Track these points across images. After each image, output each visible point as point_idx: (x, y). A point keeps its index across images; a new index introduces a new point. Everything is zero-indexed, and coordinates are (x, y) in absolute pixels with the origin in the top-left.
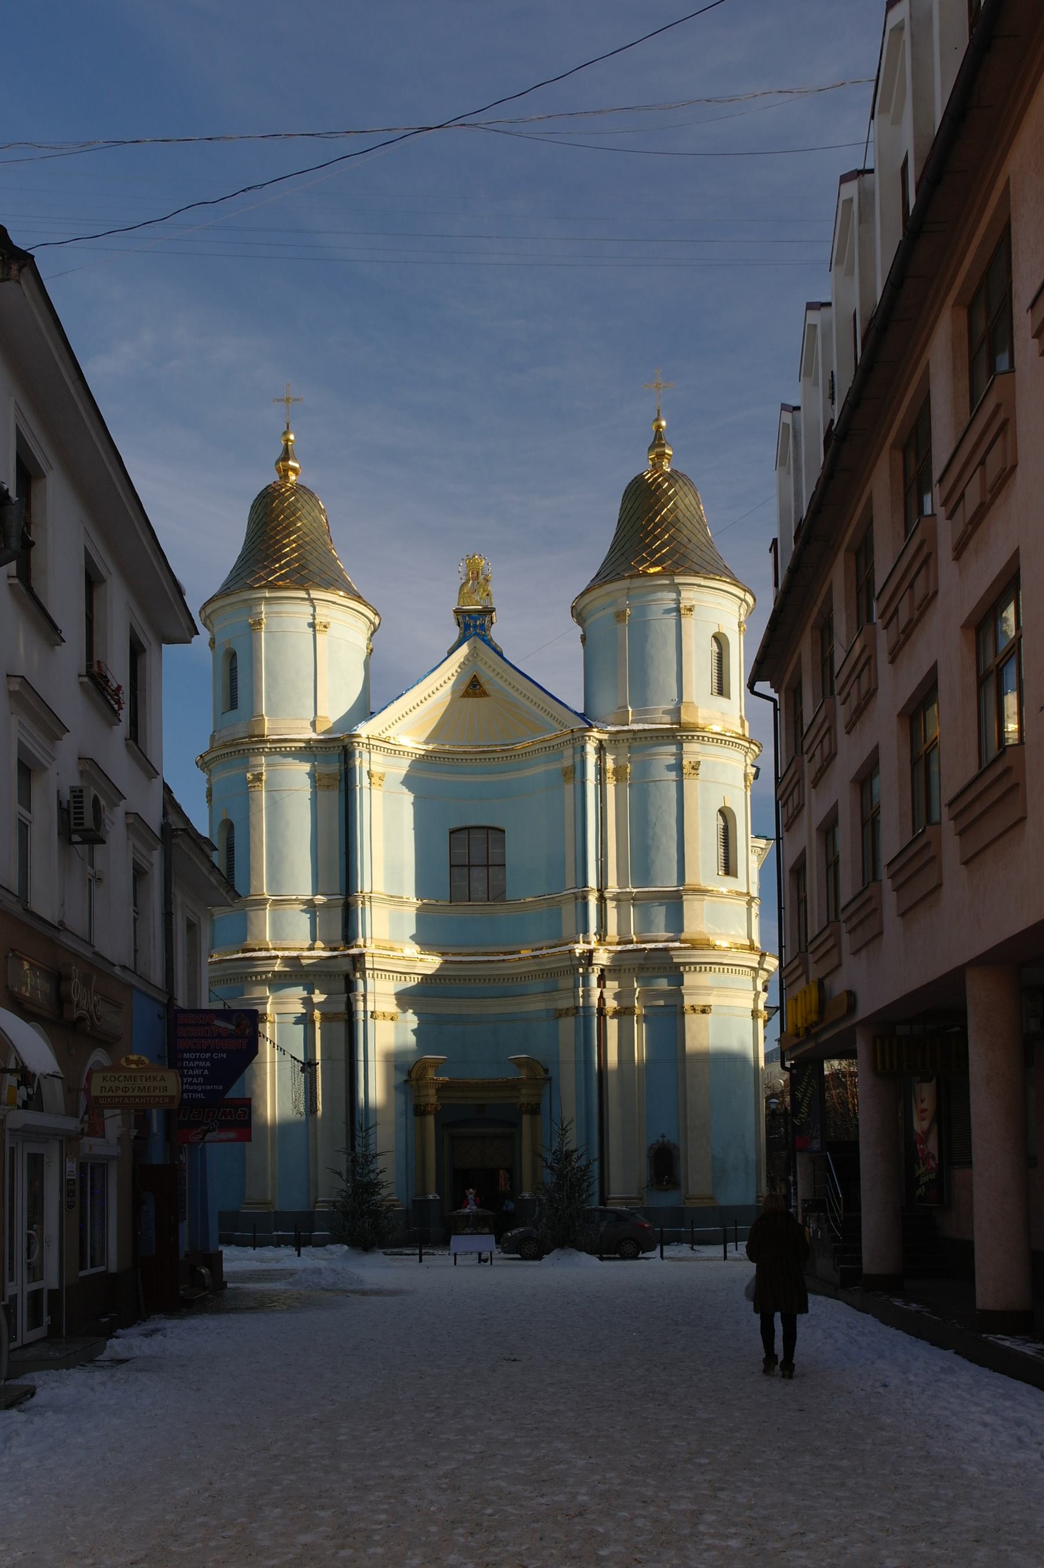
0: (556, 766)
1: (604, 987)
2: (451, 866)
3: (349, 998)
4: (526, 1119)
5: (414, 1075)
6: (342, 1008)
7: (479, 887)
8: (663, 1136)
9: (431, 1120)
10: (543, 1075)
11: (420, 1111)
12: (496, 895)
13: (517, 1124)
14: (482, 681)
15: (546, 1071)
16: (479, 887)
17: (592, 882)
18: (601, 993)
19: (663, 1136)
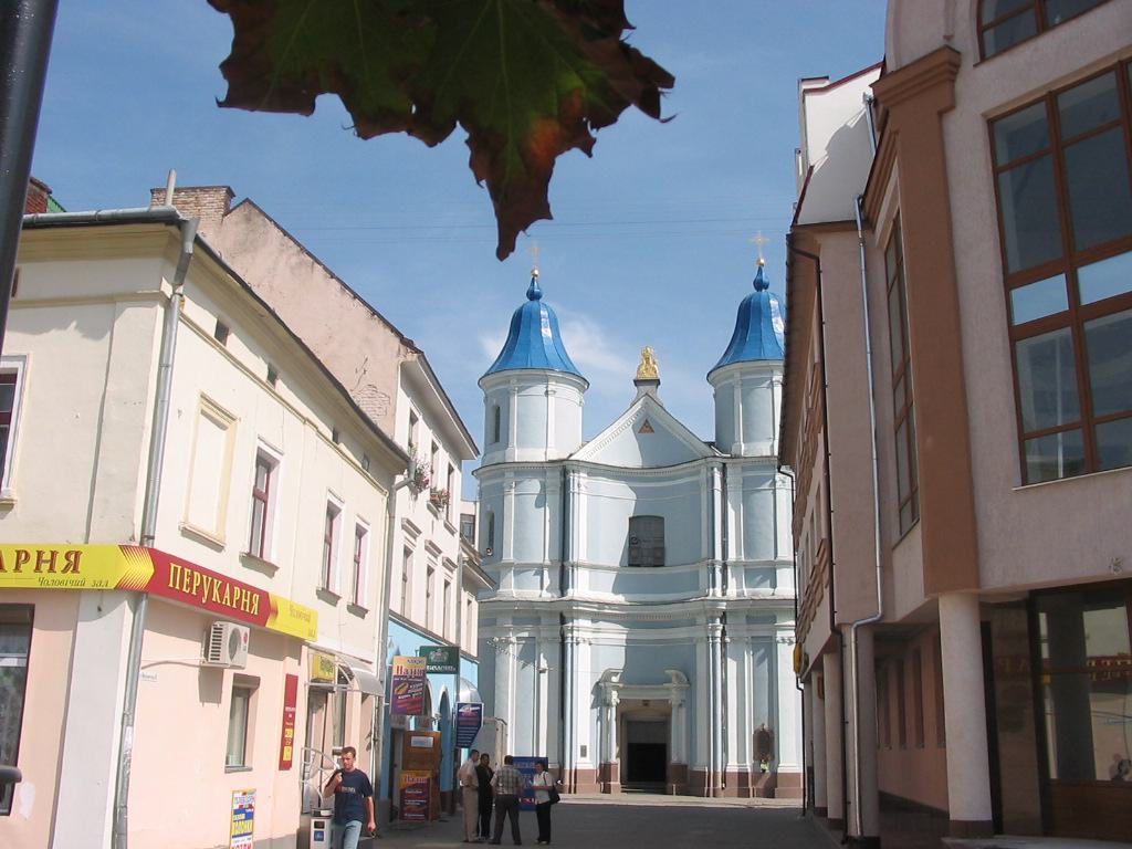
17: (718, 556)
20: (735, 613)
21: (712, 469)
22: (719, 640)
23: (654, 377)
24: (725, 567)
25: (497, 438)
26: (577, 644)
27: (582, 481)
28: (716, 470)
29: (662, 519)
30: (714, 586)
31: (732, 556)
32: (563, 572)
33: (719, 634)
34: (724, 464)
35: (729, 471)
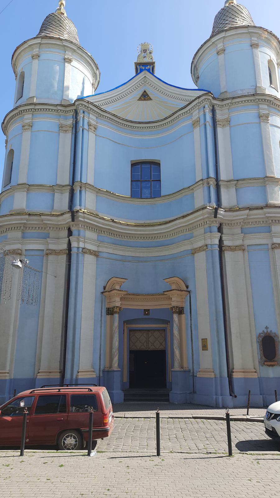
0: (189, 122)
1: (222, 233)
2: (132, 181)
3: (69, 241)
4: (175, 317)
5: (106, 289)
6: (65, 246)
7: (146, 192)
8: (267, 328)
9: (116, 316)
10: (185, 289)
11: (110, 312)
12: (156, 194)
13: (168, 322)
14: (148, 93)
15: (187, 287)
16: (146, 192)
18: (221, 237)
19: (267, 328)
20: (231, 224)
21: (204, 107)
22: (217, 248)
23: (150, 61)
24: (218, 187)
25: (22, 97)
26: (85, 253)
27: (93, 122)
28: (207, 106)
29: (157, 164)
30: (210, 202)
31: (223, 176)
32: (73, 189)
33: (217, 242)
34: (213, 106)
35: (217, 111)
